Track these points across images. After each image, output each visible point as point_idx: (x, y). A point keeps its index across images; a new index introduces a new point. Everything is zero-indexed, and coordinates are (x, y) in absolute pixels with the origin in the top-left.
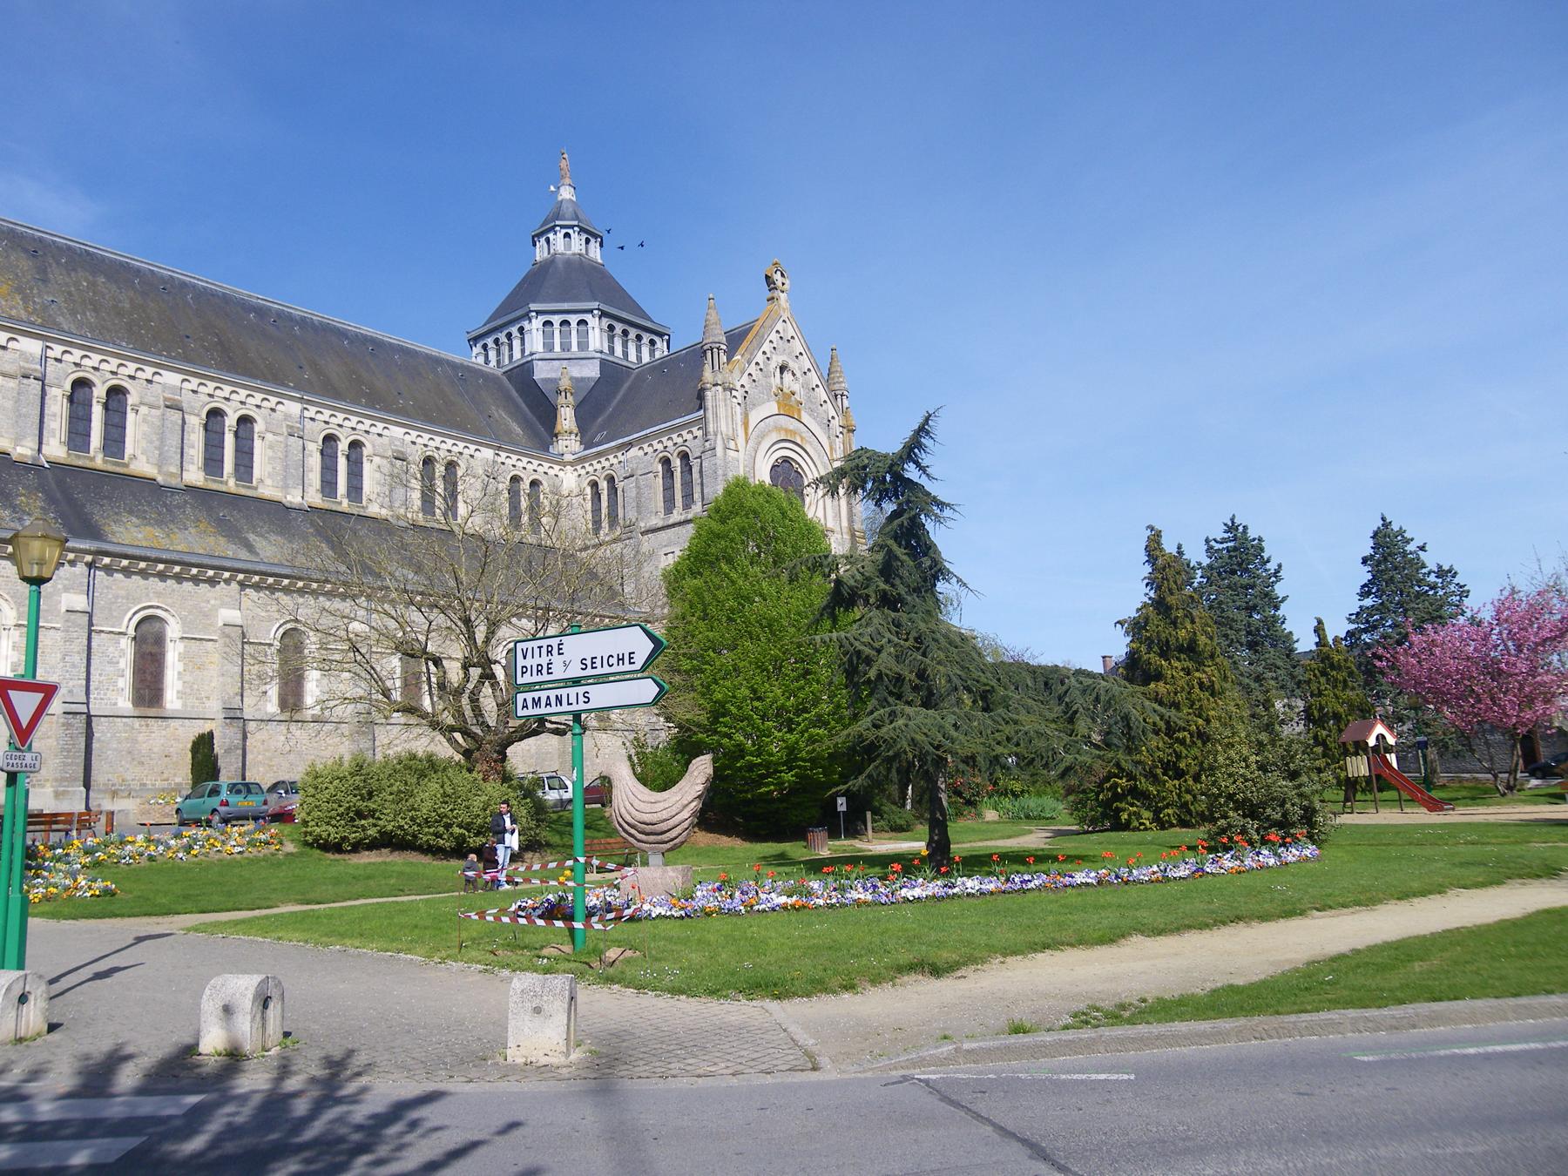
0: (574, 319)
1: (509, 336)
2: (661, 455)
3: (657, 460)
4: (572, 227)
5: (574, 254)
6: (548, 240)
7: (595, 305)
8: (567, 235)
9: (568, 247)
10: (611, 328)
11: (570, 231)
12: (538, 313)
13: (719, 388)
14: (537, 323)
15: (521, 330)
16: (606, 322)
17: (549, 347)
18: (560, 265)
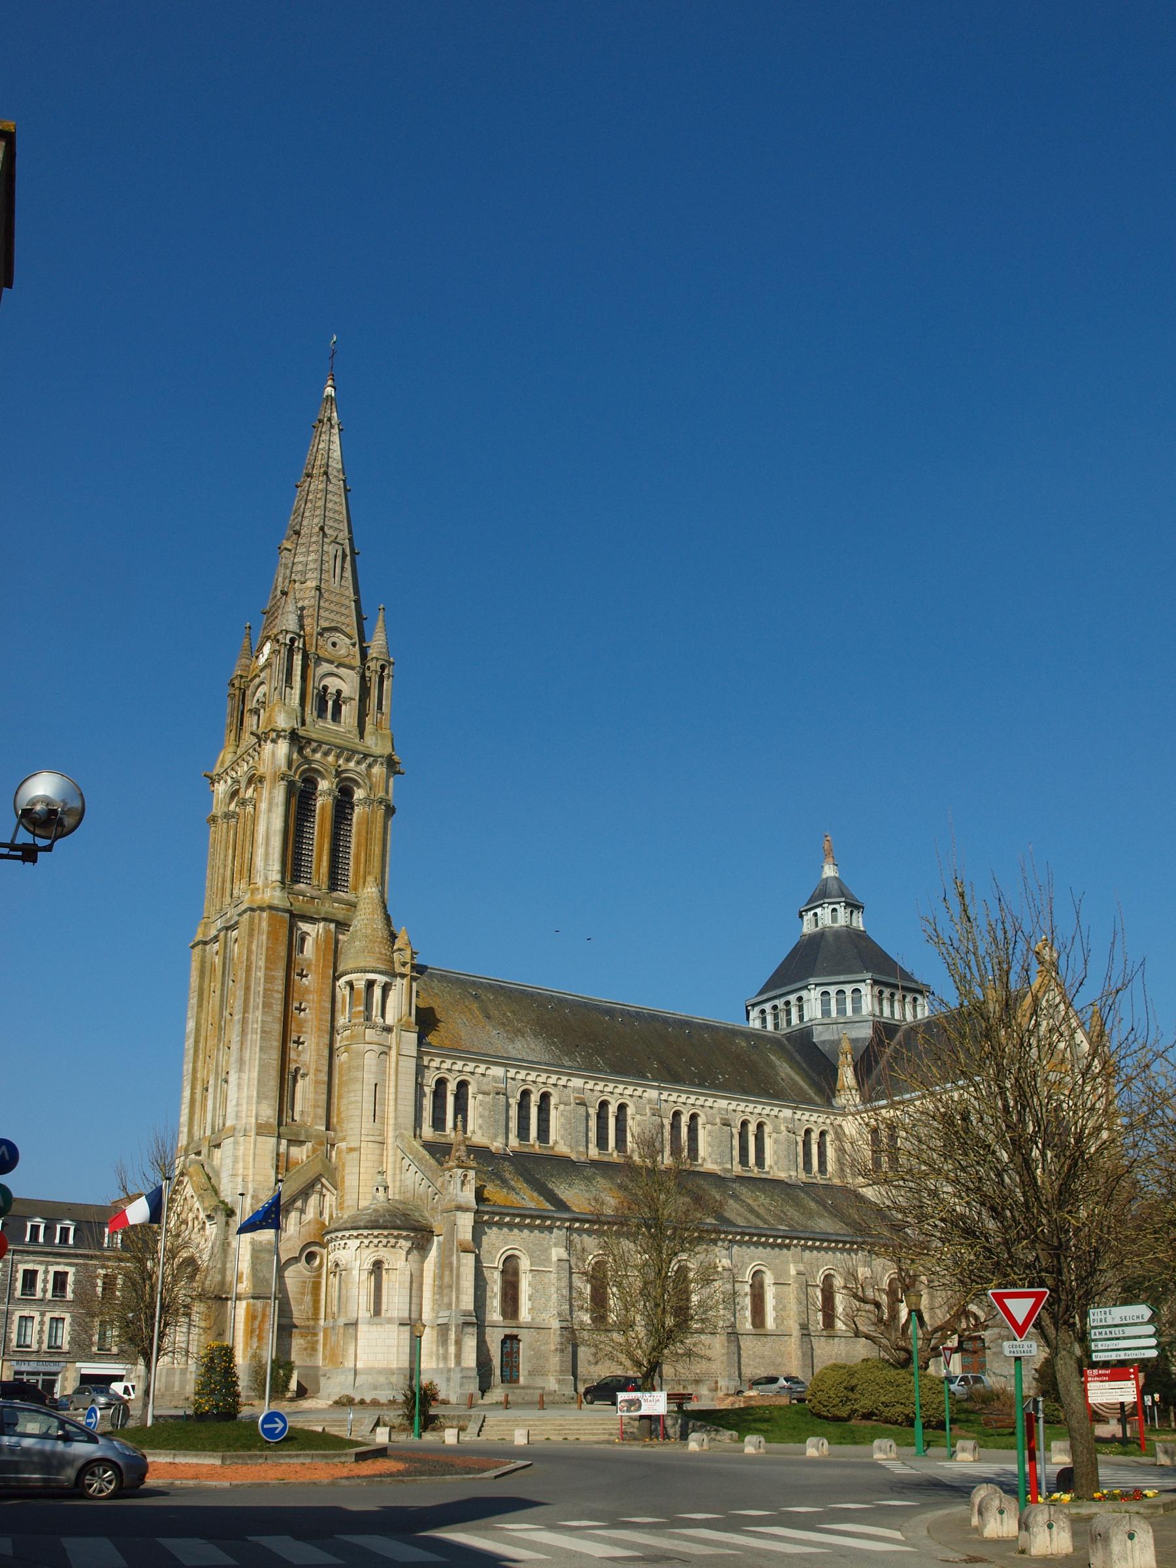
0: (848, 989)
4: (839, 903)
5: (841, 926)
6: (815, 915)
8: (834, 910)
9: (834, 919)
10: (881, 992)
12: (816, 985)
15: (800, 999)
16: (876, 989)
17: (826, 1012)
18: (831, 939)
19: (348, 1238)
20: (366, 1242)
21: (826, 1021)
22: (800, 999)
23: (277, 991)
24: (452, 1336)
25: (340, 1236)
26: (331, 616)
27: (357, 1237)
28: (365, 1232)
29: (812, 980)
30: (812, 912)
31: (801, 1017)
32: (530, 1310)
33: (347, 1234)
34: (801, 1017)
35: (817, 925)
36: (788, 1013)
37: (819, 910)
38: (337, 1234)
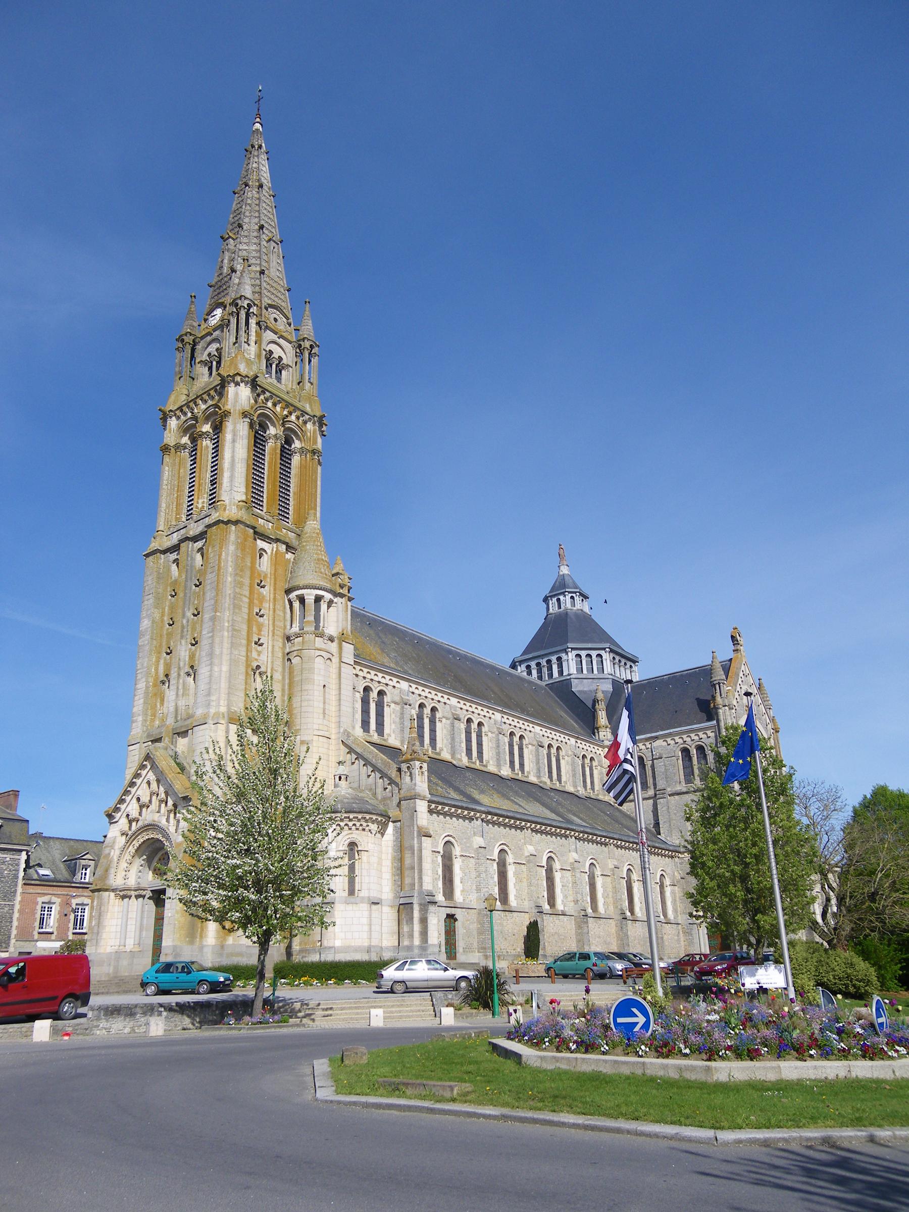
1: (549, 662)
2: (682, 746)
3: (679, 749)
4: (575, 593)
5: (578, 610)
6: (559, 600)
7: (607, 645)
8: (572, 598)
9: (573, 604)
11: (574, 595)
12: (572, 649)
13: (727, 708)
14: (572, 655)
15: (559, 659)
17: (581, 670)
21: (580, 676)
23: (245, 596)
24: (416, 914)
26: (272, 297)
29: (570, 645)
31: (561, 673)
32: (462, 891)
34: (561, 673)
35: (560, 607)
36: (550, 669)
37: (561, 597)
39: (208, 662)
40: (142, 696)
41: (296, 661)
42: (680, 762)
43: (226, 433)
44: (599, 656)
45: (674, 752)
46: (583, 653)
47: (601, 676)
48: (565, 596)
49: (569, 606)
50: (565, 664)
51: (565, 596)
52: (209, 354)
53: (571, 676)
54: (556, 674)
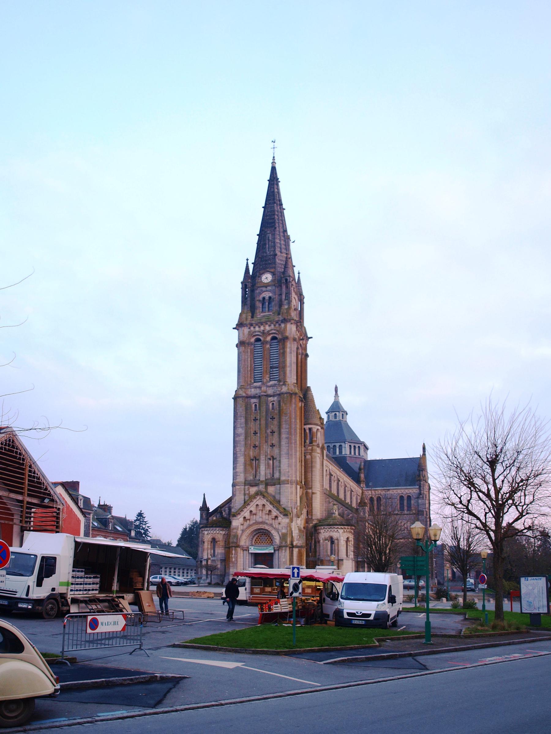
1: (335, 446)
2: (400, 495)
6: (335, 414)
8: (343, 414)
11: (343, 413)
13: (424, 481)
15: (340, 446)
19: (339, 529)
20: (345, 530)
21: (350, 456)
22: (340, 446)
25: (336, 527)
27: (342, 528)
28: (346, 527)
30: (334, 413)
33: (340, 527)
34: (341, 452)
37: (337, 413)
38: (334, 526)
39: (288, 457)
40: (242, 465)
41: (308, 457)
42: (399, 501)
43: (287, 348)
44: (359, 447)
45: (397, 496)
46: (352, 445)
47: (359, 457)
48: (339, 413)
49: (341, 418)
50: (343, 449)
51: (339, 413)
52: (264, 298)
53: (347, 455)
54: (338, 453)
